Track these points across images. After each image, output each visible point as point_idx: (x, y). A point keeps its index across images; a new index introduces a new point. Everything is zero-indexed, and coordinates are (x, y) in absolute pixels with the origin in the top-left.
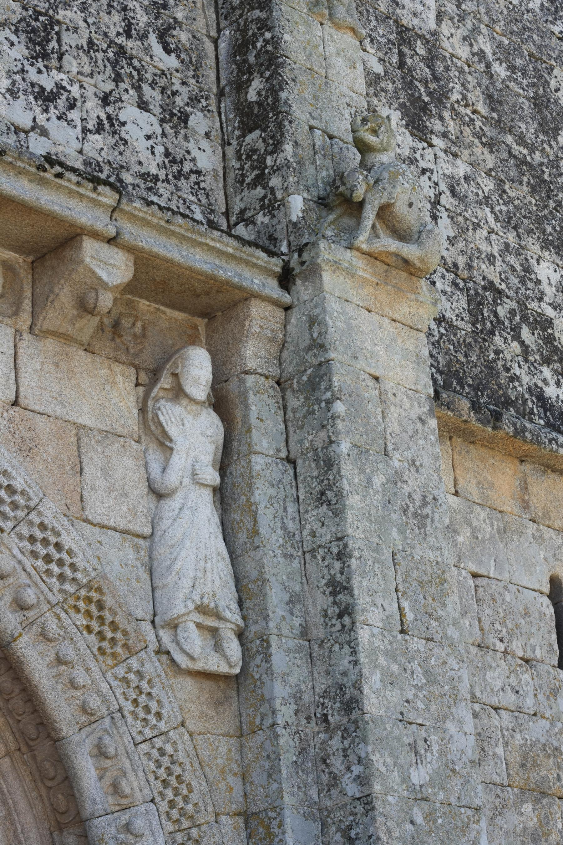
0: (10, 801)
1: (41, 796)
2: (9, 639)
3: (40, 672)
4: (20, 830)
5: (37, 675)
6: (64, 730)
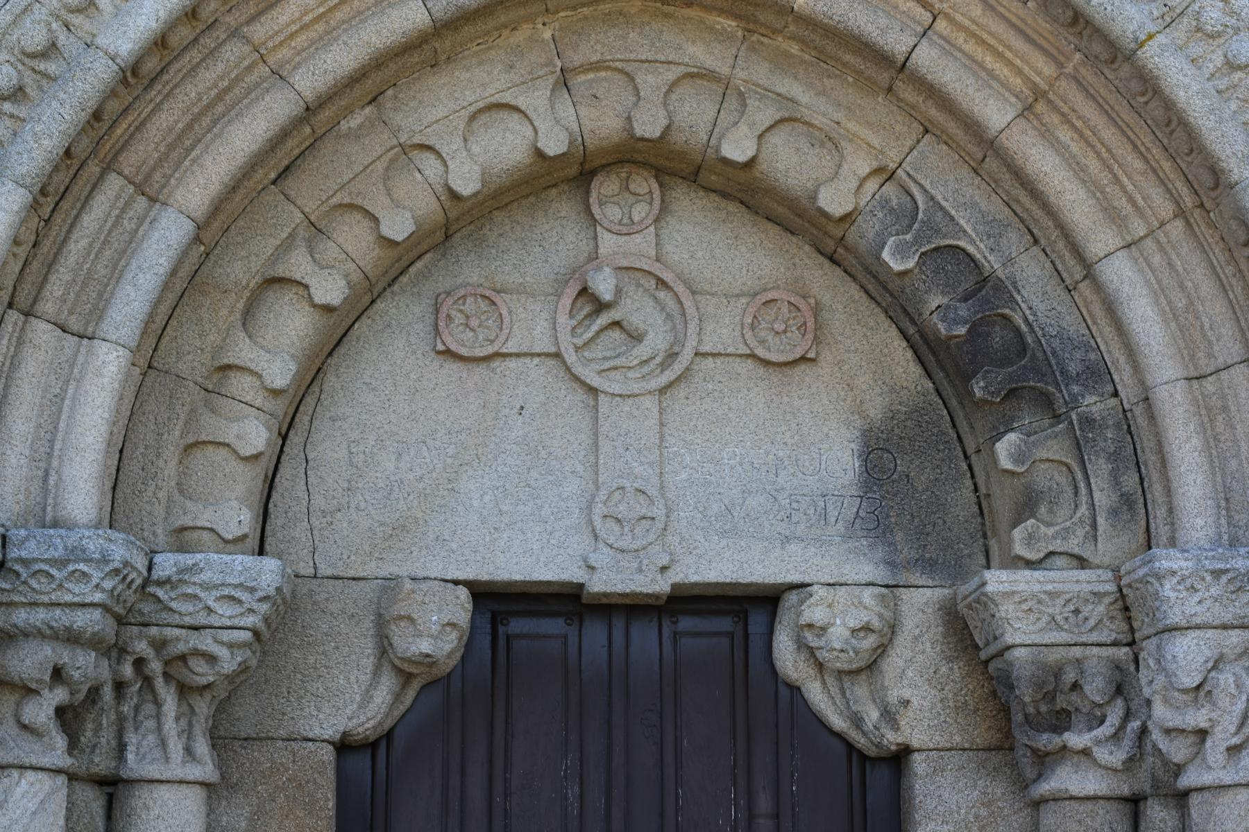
0: (1190, 284)
1: (1240, 271)
2: (1132, 45)
3: (1187, 88)
4: (1207, 326)
5: (1182, 93)
6: (1236, 170)
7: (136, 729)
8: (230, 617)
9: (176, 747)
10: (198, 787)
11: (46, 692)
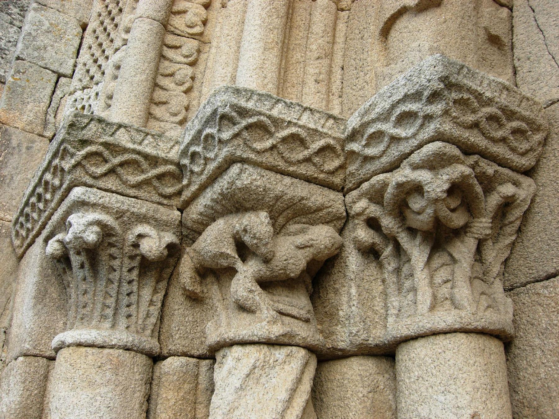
7: (399, 290)
8: (414, 135)
9: (425, 296)
10: (462, 337)
11: (239, 265)
